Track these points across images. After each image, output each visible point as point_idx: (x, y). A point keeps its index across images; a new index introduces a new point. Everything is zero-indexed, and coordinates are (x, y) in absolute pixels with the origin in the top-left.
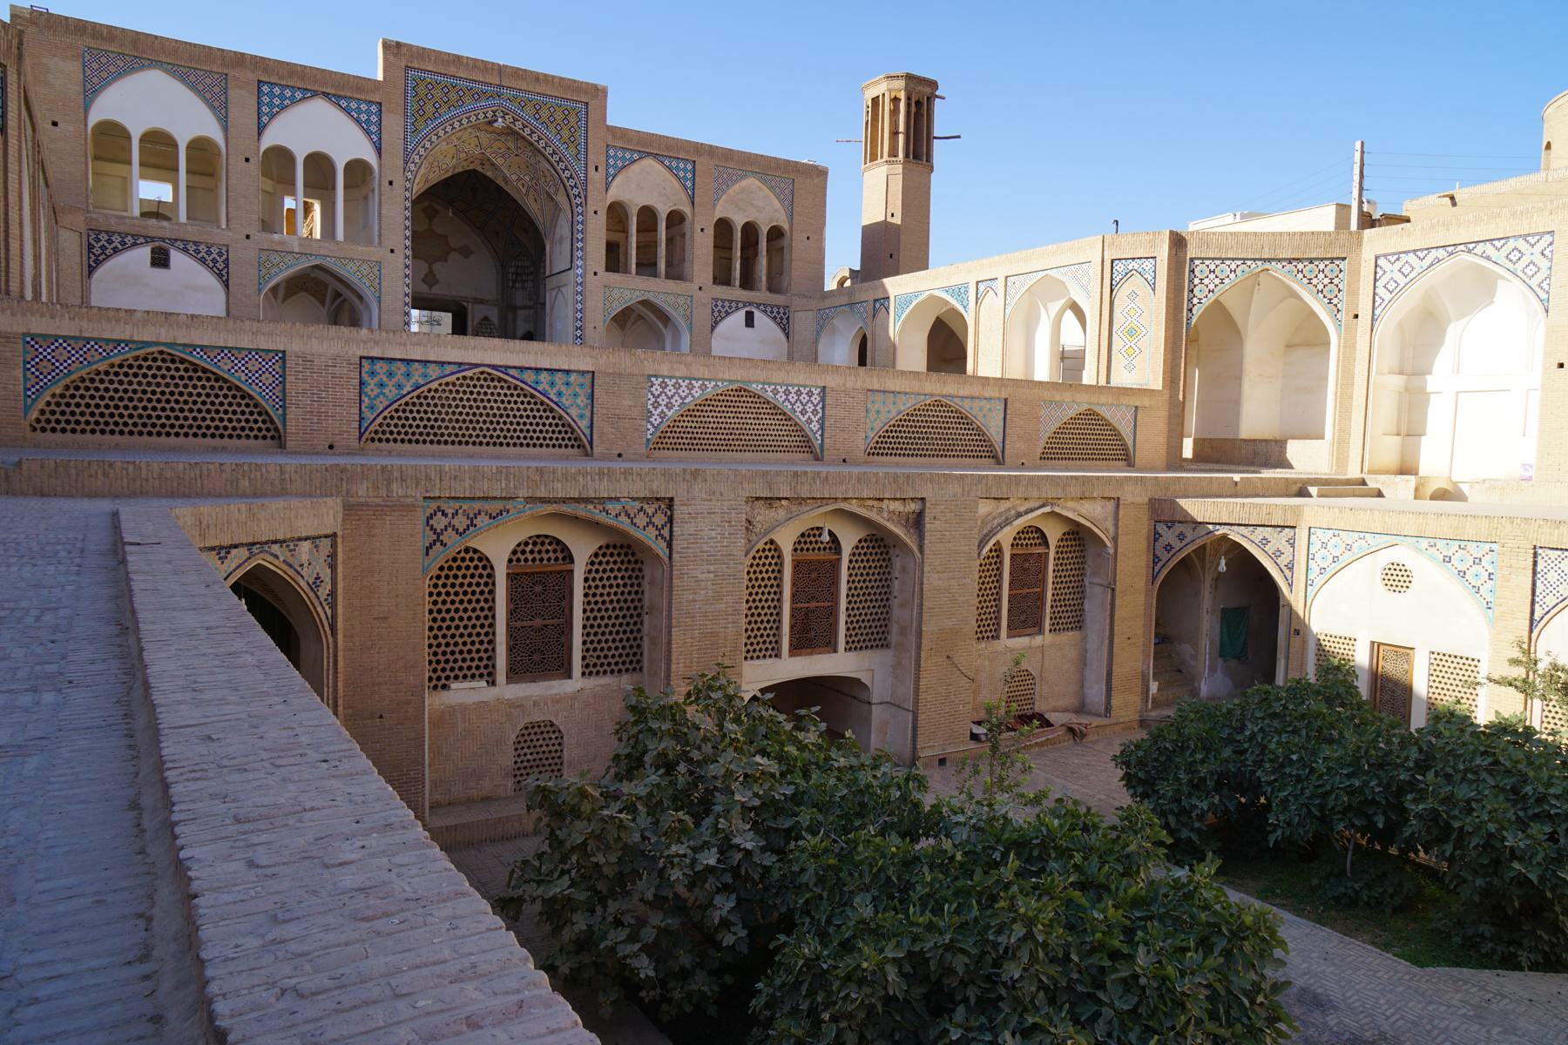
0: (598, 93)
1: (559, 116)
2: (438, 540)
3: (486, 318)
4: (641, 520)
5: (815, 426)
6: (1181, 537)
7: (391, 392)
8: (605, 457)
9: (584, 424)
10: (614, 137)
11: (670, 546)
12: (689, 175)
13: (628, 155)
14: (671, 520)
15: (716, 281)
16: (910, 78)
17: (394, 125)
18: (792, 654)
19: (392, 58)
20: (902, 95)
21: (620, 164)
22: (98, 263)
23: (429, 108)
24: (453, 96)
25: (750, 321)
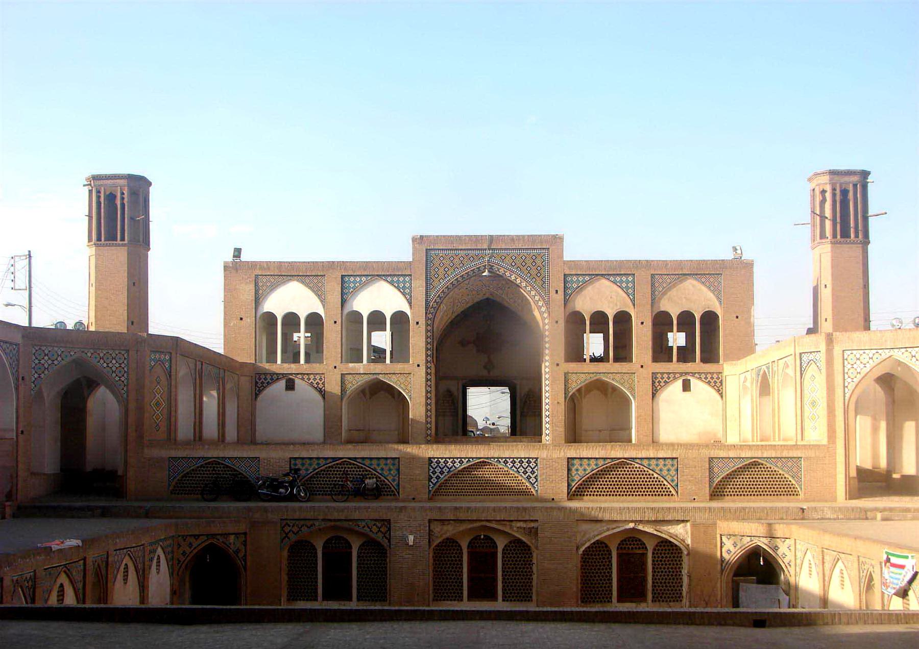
0: (557, 240)
1: (529, 262)
4: (375, 529)
5: (533, 480)
6: (735, 545)
8: (404, 501)
10: (570, 268)
11: (389, 541)
12: (630, 285)
13: (581, 279)
14: (389, 529)
15: (655, 359)
16: (833, 173)
17: (419, 286)
18: (469, 600)
19: (417, 246)
20: (828, 188)
22: (260, 391)
24: (457, 261)
25: (686, 387)
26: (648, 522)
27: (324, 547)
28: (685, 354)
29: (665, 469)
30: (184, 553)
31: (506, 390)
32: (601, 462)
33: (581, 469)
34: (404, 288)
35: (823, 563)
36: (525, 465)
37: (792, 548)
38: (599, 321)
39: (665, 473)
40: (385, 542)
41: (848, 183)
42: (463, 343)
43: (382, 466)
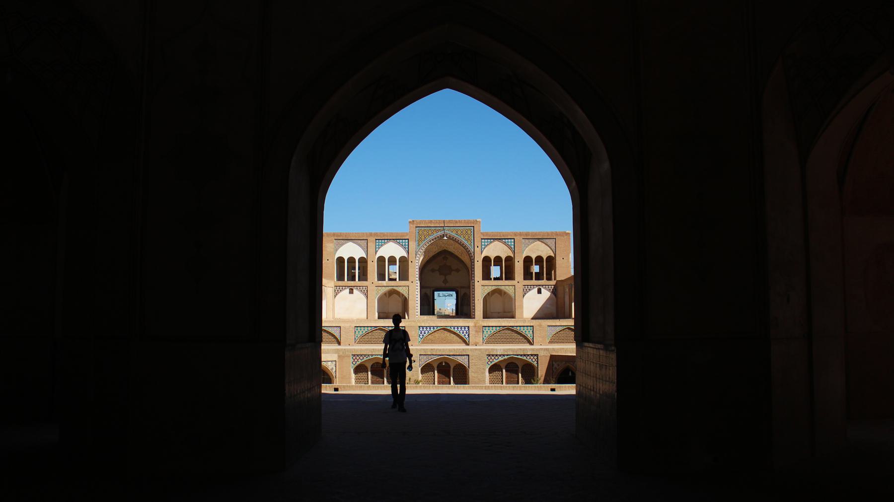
17: (413, 245)
25: (539, 292)
28: (539, 276)
31: (454, 293)
38: (498, 260)
42: (433, 271)
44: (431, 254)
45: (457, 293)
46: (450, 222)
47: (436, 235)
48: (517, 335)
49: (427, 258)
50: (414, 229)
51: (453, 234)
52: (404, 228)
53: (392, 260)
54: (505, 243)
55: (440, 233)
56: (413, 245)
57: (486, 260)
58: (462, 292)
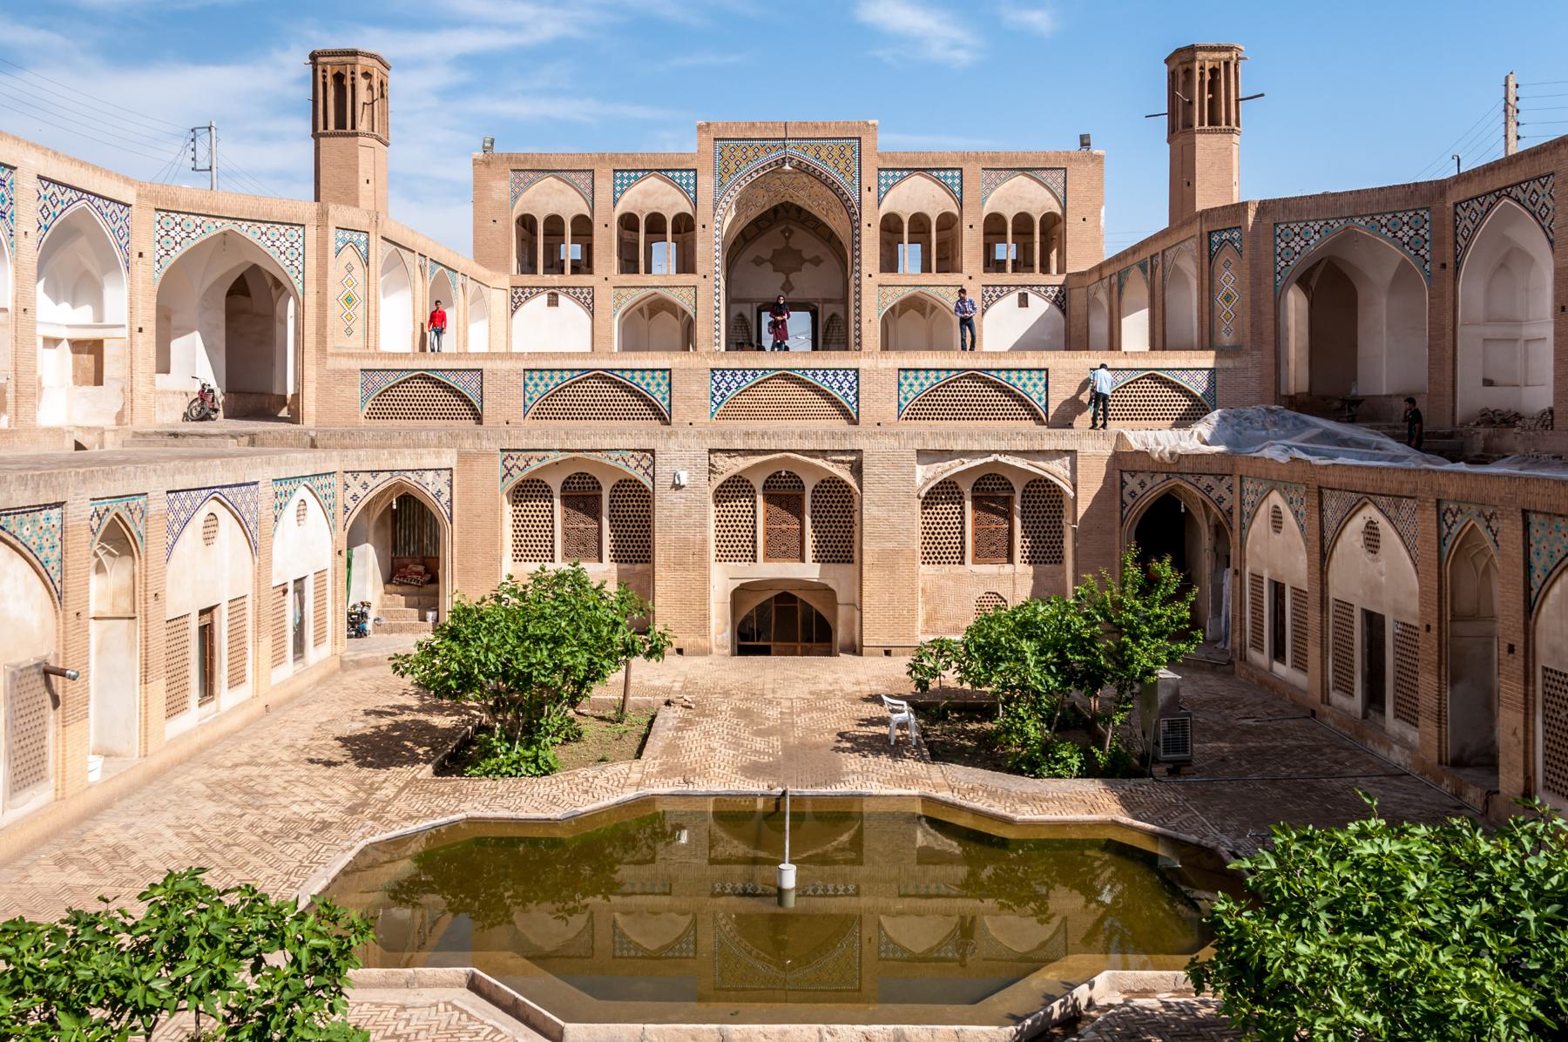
2: (509, 473)
3: (834, 315)
4: (633, 463)
5: (851, 399)
7: (542, 389)
9: (665, 403)
12: (957, 181)
13: (898, 174)
14: (654, 463)
17: (707, 184)
21: (891, 182)
23: (732, 166)
24: (750, 153)
25: (1023, 301)
26: (1017, 453)
27: (563, 489)
29: (1030, 384)
30: (355, 497)
32: (943, 375)
33: (917, 383)
34: (688, 184)
35: (1321, 510)
36: (841, 378)
37: (1237, 490)
38: (920, 224)
39: (1029, 389)
40: (647, 481)
41: (1219, 60)
42: (758, 261)
43: (648, 379)
44: (754, 213)
45: (815, 315)
46: (800, 126)
47: (764, 159)
48: (995, 391)
49: (743, 222)
50: (709, 145)
51: (809, 158)
52: (682, 143)
53: (656, 224)
54: (937, 180)
55: (774, 155)
56: (707, 184)
57: (891, 225)
58: (826, 312)
